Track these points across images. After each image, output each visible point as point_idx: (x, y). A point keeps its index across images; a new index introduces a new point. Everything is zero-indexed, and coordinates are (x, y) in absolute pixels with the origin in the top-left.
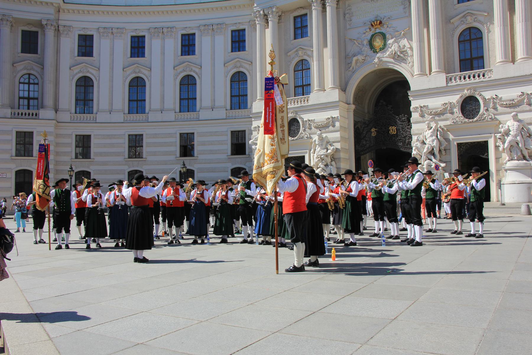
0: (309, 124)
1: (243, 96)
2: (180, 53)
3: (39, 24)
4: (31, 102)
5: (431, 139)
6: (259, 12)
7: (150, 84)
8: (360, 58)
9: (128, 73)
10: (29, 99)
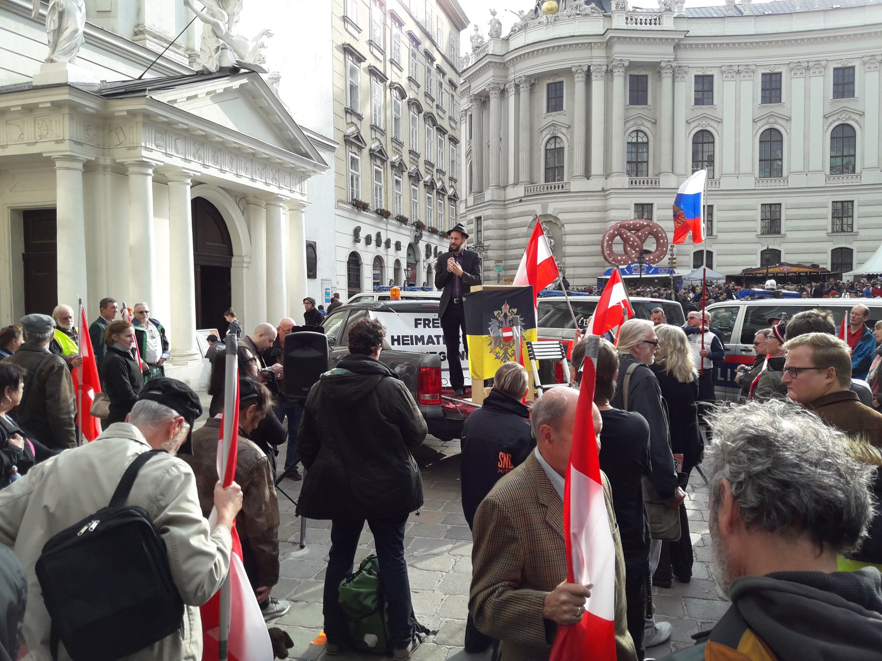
2: (831, 96)
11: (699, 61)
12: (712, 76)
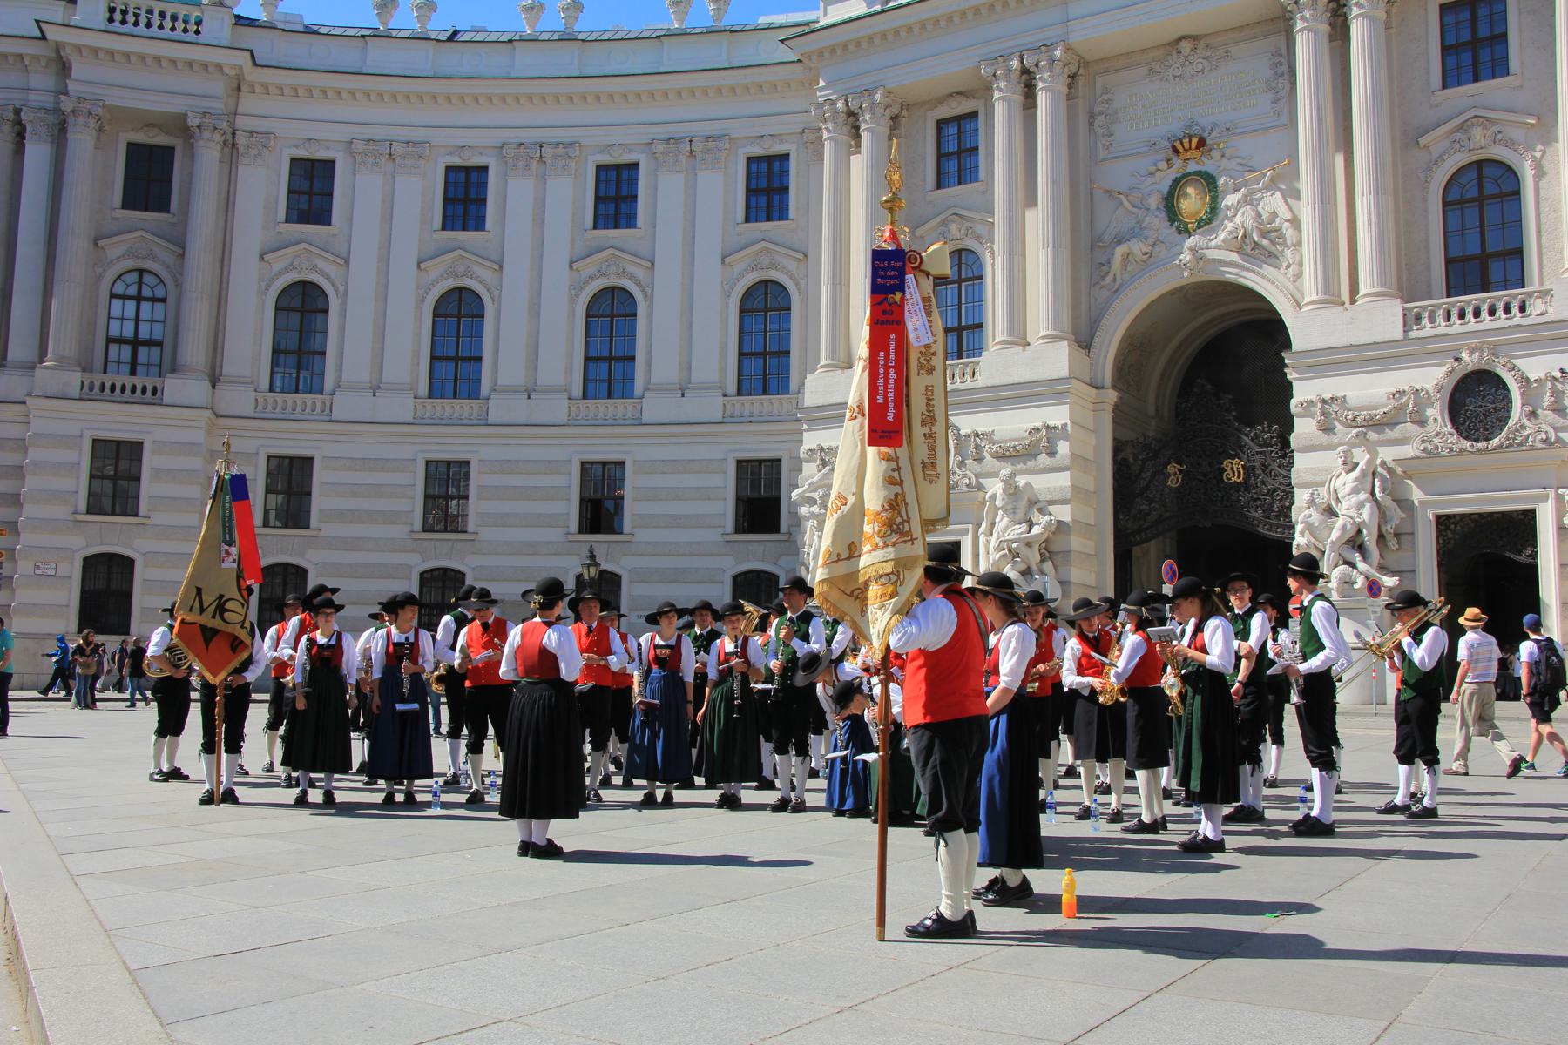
0: (977, 447)
1: (777, 354)
3: (181, 126)
4: (143, 352)
5: (1354, 499)
6: (833, 103)
7: (498, 312)
8: (1137, 247)
9: (433, 274)
10: (135, 343)
11: (298, 123)
12: (332, 163)
